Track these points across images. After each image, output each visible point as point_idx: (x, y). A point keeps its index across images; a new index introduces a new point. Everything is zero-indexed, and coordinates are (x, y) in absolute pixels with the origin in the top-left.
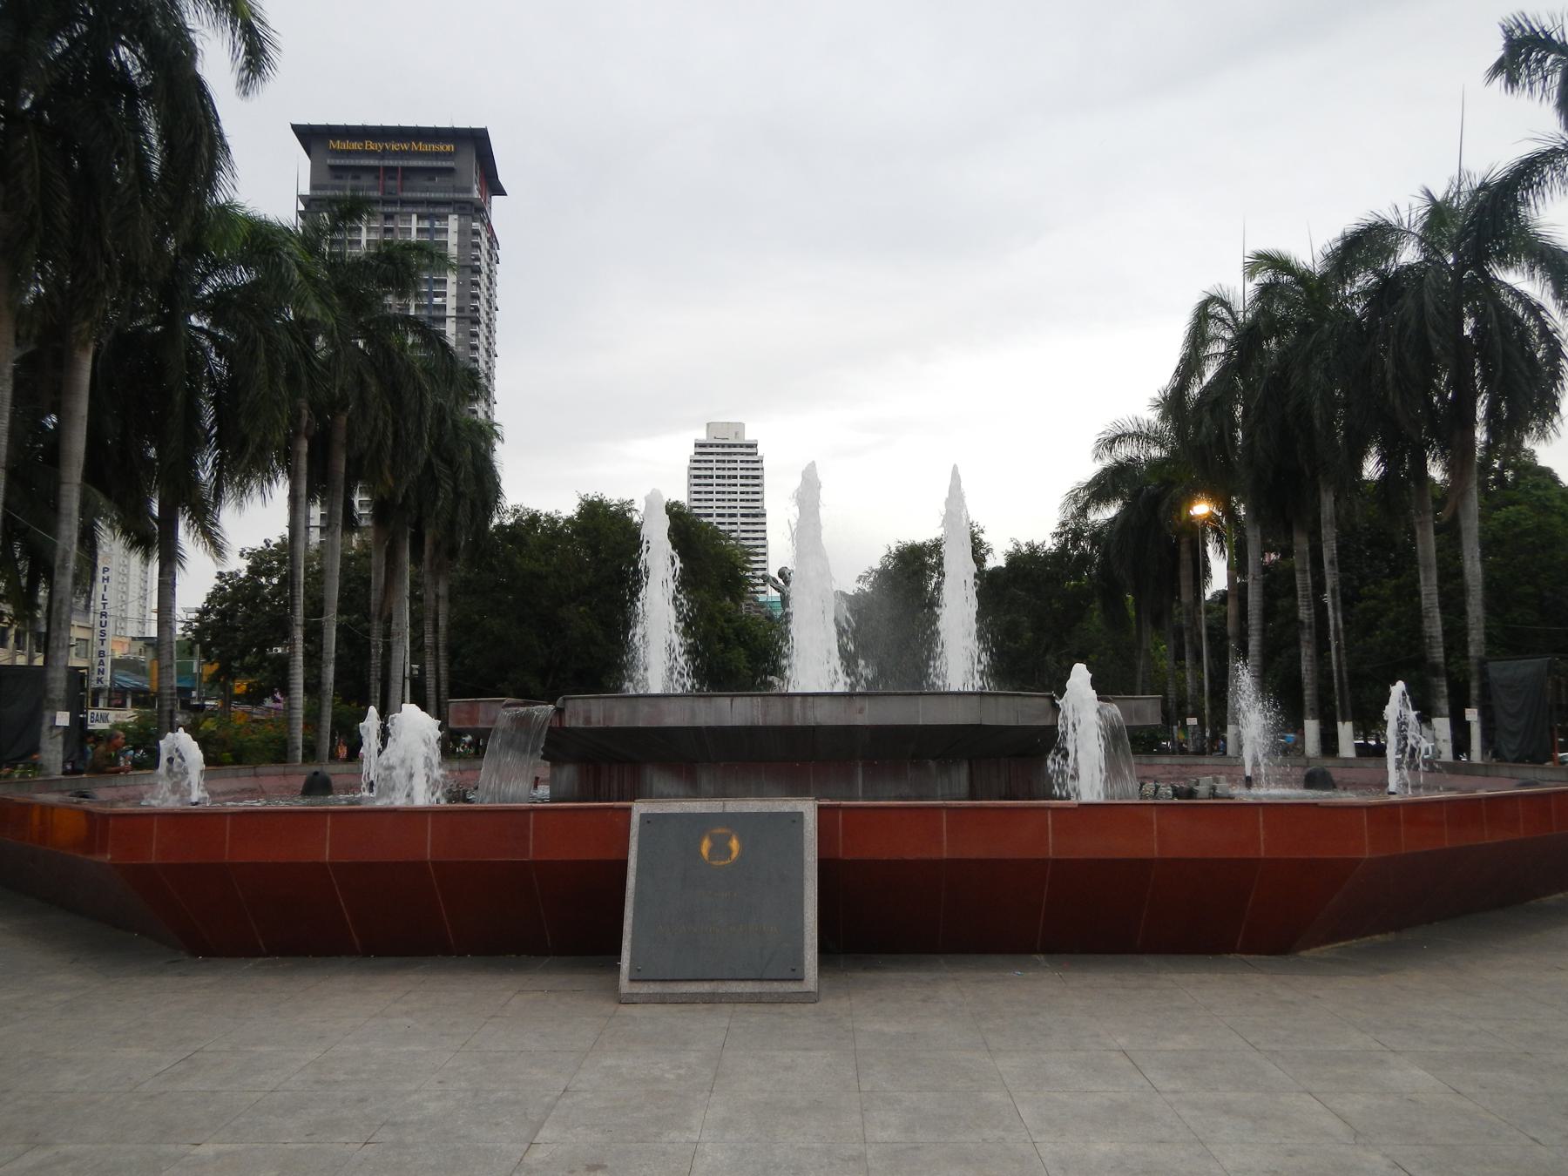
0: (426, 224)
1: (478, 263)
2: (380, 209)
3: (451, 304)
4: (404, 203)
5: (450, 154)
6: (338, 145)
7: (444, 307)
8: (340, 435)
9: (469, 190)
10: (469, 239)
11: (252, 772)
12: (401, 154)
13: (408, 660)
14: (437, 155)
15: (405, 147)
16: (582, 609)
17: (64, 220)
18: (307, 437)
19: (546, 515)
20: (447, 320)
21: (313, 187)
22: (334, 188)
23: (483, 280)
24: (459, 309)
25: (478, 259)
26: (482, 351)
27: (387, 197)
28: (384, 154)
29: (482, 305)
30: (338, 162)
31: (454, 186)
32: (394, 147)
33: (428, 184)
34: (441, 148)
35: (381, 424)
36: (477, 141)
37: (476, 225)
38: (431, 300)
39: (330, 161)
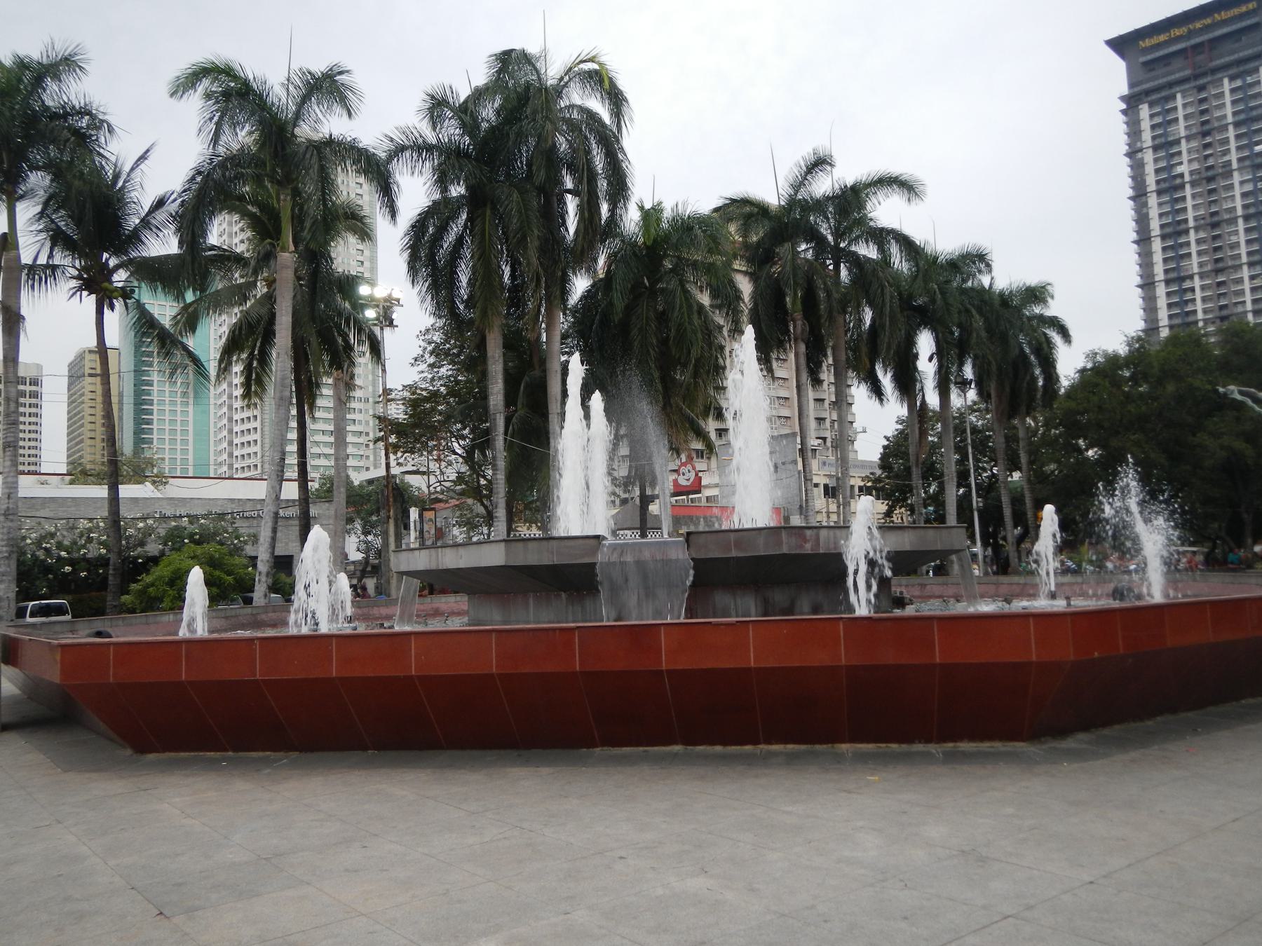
0: (1238, 83)
2: (1193, 84)
4: (1214, 71)
6: (1148, 43)
12: (1207, 28)
14: (1241, 17)
15: (1208, 21)
18: (803, 340)
21: (1132, 85)
22: (1148, 80)
27: (1198, 71)
28: (1191, 34)
30: (1149, 57)
32: (1198, 25)
33: (1237, 45)
34: (1244, 9)
38: (1252, 150)
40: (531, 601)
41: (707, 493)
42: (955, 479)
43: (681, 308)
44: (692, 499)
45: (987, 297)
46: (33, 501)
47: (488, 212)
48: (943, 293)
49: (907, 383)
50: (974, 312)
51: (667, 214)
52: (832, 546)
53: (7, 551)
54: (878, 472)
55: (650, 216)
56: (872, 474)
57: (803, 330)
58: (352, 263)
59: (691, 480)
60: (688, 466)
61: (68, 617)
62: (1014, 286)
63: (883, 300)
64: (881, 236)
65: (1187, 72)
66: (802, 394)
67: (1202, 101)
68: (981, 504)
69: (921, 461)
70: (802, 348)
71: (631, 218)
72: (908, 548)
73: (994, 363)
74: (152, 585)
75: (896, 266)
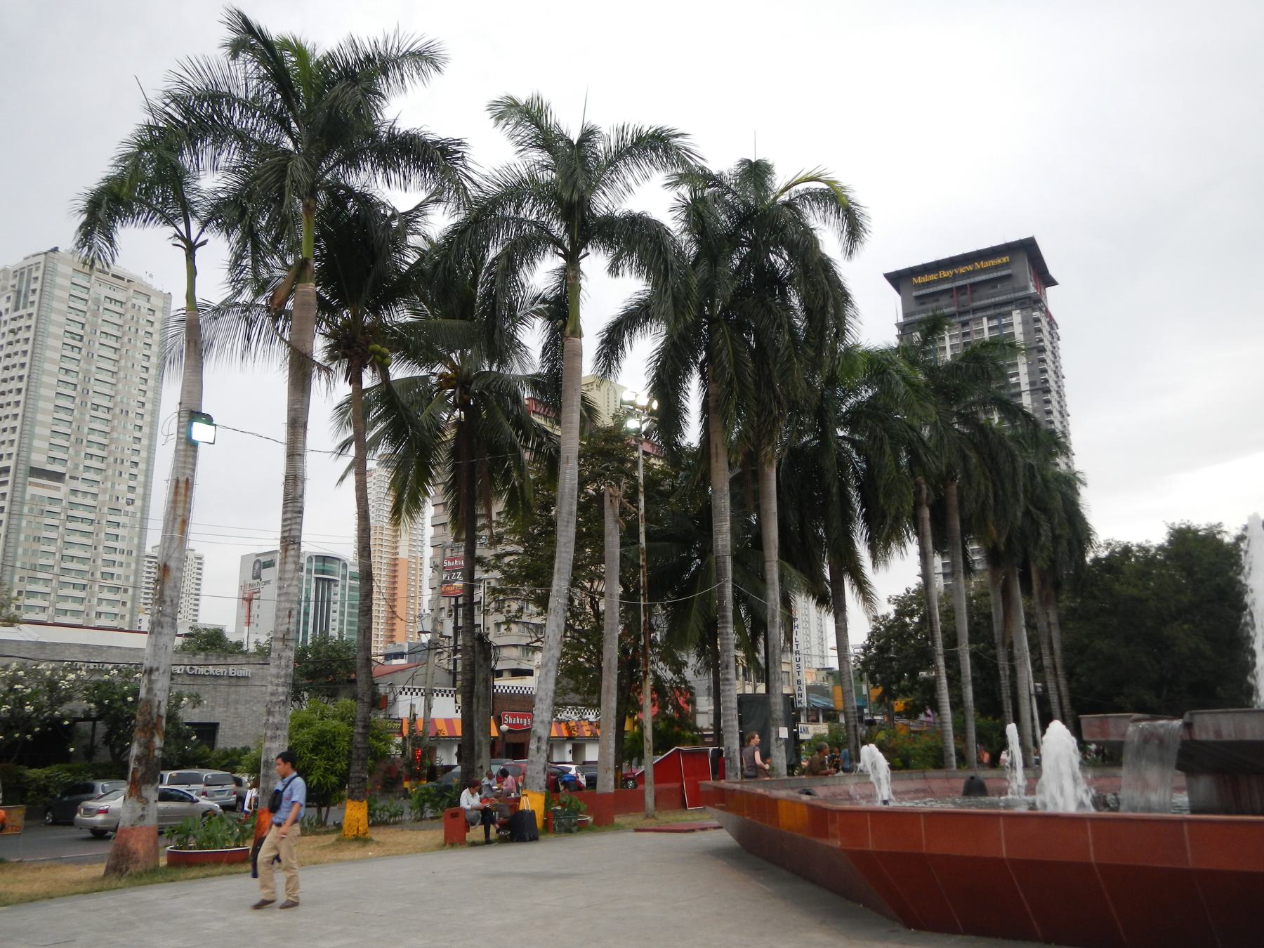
0: (995, 323)
1: (1041, 344)
2: (958, 319)
3: (1024, 381)
4: (975, 310)
5: (1007, 264)
6: (920, 280)
7: (1018, 385)
8: (954, 501)
9: (1026, 288)
10: (1032, 327)
11: (922, 775)
12: (968, 274)
13: (1031, 679)
14: (997, 268)
15: (970, 268)
16: (1186, 627)
17: (750, 379)
18: (928, 506)
19: (1139, 546)
20: (1023, 394)
21: (905, 315)
22: (919, 313)
23: (1048, 356)
24: (1032, 383)
25: (1041, 340)
26: (1056, 413)
27: (962, 309)
28: (955, 277)
29: (1050, 376)
30: (921, 292)
31: (1014, 288)
32: (962, 270)
33: (992, 291)
34: (999, 261)
35: (983, 488)
36: (1027, 250)
37: (1036, 314)
39: (915, 294)
53: (283, 693)
58: (131, 402)
63: (1014, 469)
65: (953, 309)
67: (965, 335)
68: (1040, 690)
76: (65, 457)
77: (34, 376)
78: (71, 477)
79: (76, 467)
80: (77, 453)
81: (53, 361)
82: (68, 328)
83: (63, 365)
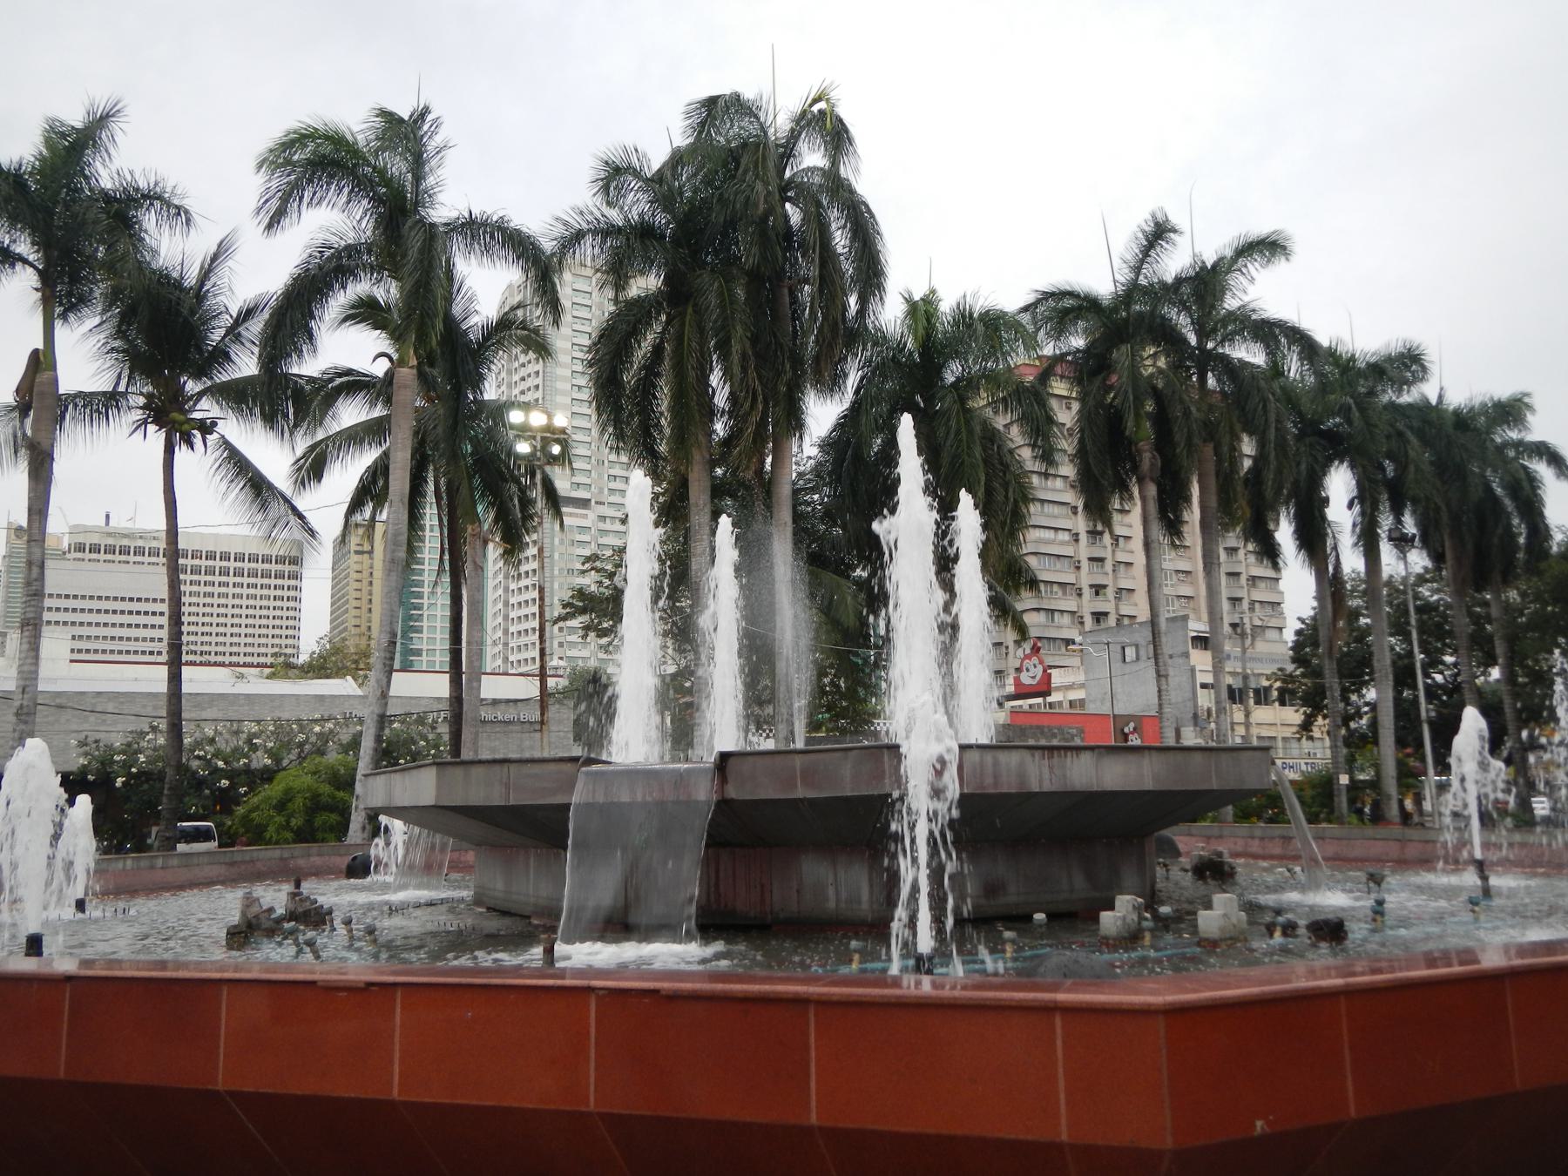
18: (1152, 479)
40: (532, 860)
41: (1055, 697)
42: (1391, 677)
43: (958, 432)
44: (1050, 704)
45: (1434, 415)
46: (199, 698)
47: (690, 310)
48: (1362, 409)
49: (1313, 538)
50: (1409, 434)
51: (946, 306)
52: (989, 781)
54: (1290, 667)
55: (921, 311)
56: (1280, 669)
57: (1152, 465)
59: (1038, 678)
60: (1035, 660)
61: (213, 845)
62: (1477, 402)
63: (1266, 420)
64: (1268, 332)
66: (1152, 554)
68: (1433, 714)
69: (1335, 649)
70: (1152, 490)
71: (890, 314)
72: (1148, 785)
73: (1444, 508)
74: (256, 808)
75: (1292, 374)
76: (588, 481)
77: (548, 397)
78: (597, 503)
79: (601, 491)
80: (600, 476)
81: (564, 379)
82: (575, 341)
83: (575, 381)
